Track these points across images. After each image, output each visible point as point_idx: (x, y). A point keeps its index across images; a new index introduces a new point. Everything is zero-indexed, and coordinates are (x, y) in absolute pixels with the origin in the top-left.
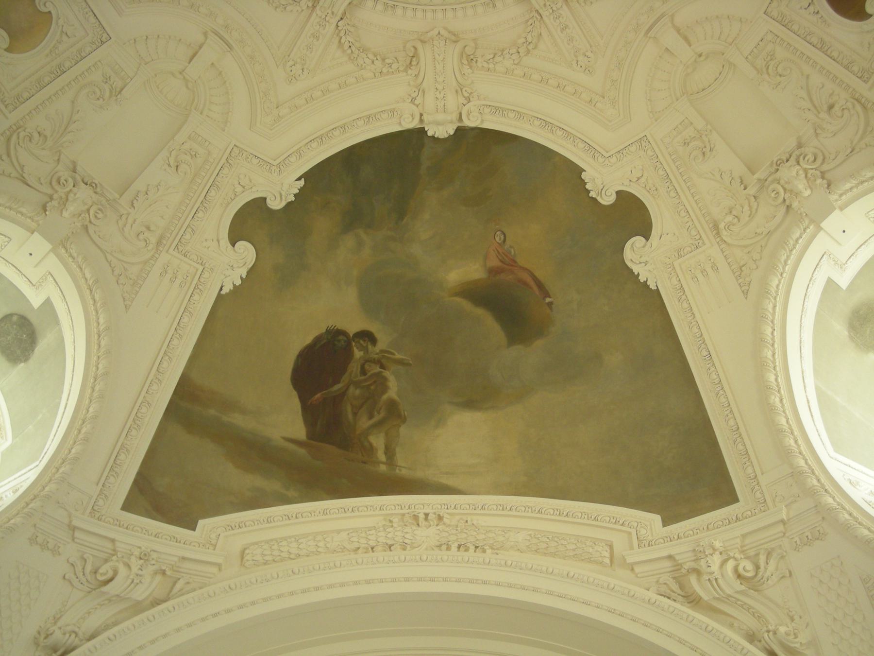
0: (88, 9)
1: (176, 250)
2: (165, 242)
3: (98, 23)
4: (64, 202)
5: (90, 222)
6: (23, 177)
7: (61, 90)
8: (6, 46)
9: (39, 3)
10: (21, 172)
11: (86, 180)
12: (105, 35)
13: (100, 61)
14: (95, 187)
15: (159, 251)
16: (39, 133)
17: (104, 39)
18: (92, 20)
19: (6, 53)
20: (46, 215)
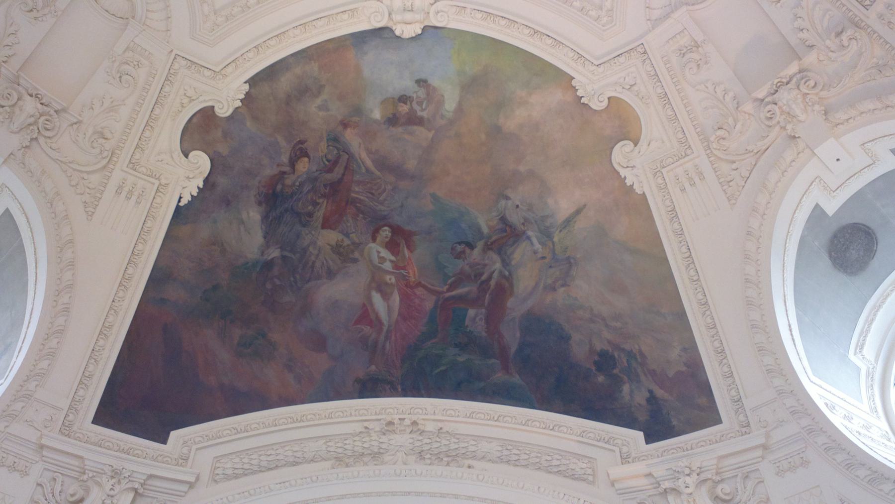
0: (612, 62)
1: (868, 7)
2: (857, 19)
3: (626, 54)
4: (790, 116)
5: (817, 94)
6: (757, 152)
7: (683, 100)
8: (632, 144)
9: (601, 107)
10: (752, 154)
11: (772, 91)
12: (639, 49)
13: (663, 58)
14: (782, 84)
15: (865, 27)
16: (719, 128)
17: (642, 51)
18: (622, 59)
19: (638, 145)
20: (799, 137)
